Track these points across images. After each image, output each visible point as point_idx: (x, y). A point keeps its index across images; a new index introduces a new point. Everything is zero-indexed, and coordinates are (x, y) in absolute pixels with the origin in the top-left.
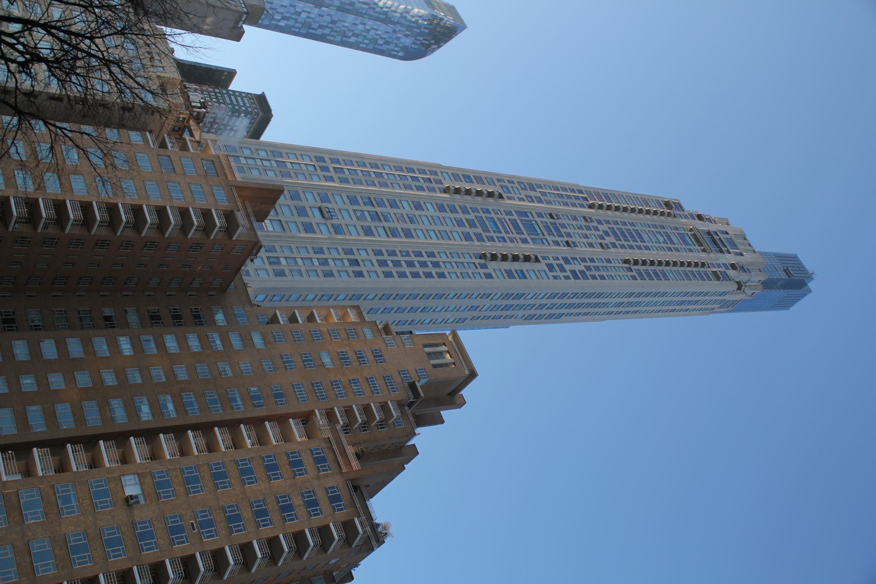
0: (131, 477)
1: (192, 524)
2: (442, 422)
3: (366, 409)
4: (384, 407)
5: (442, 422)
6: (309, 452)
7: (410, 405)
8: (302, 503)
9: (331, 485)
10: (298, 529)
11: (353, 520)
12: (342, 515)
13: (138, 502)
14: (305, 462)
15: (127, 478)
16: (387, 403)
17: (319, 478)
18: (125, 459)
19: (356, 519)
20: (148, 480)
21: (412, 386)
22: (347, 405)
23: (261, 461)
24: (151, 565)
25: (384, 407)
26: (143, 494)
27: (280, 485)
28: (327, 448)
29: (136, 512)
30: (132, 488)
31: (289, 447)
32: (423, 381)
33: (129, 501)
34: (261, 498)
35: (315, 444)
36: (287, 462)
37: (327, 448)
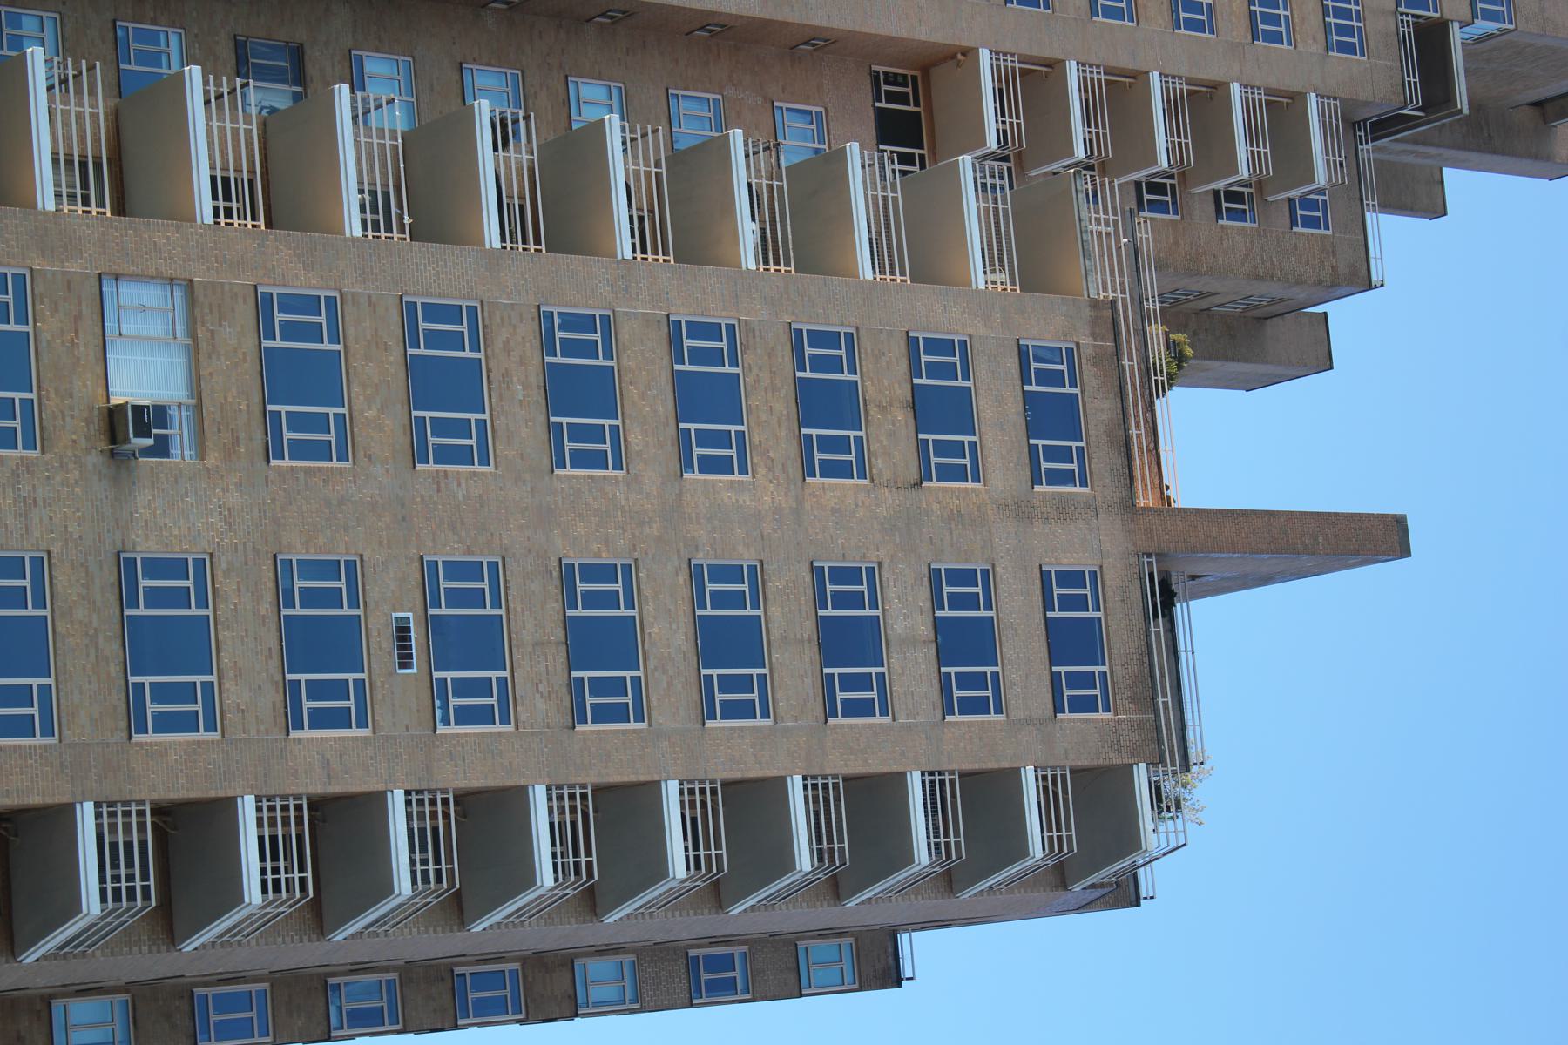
0: (151, 295)
1: (403, 631)
2: (1435, 208)
3: (1201, 104)
4: (1280, 114)
5: (1435, 208)
6: (1012, 364)
7: (1385, 126)
8: (925, 629)
9: (1069, 563)
10: (875, 766)
11: (1127, 772)
12: (1083, 737)
13: (162, 448)
14: (984, 409)
15: (131, 294)
16: (1297, 98)
17: (1024, 512)
18: (124, 174)
19: (1141, 774)
20: (237, 336)
21: (1430, 43)
22: (1125, 61)
23: (785, 356)
24: (160, 810)
25: (1280, 114)
26: (199, 407)
27: (852, 516)
28: (1098, 359)
29: (145, 501)
30: (143, 373)
31: (937, 313)
32: (1483, 26)
33: (126, 430)
34: (746, 559)
35: (1050, 324)
36: (904, 392)
37: (1098, 359)
